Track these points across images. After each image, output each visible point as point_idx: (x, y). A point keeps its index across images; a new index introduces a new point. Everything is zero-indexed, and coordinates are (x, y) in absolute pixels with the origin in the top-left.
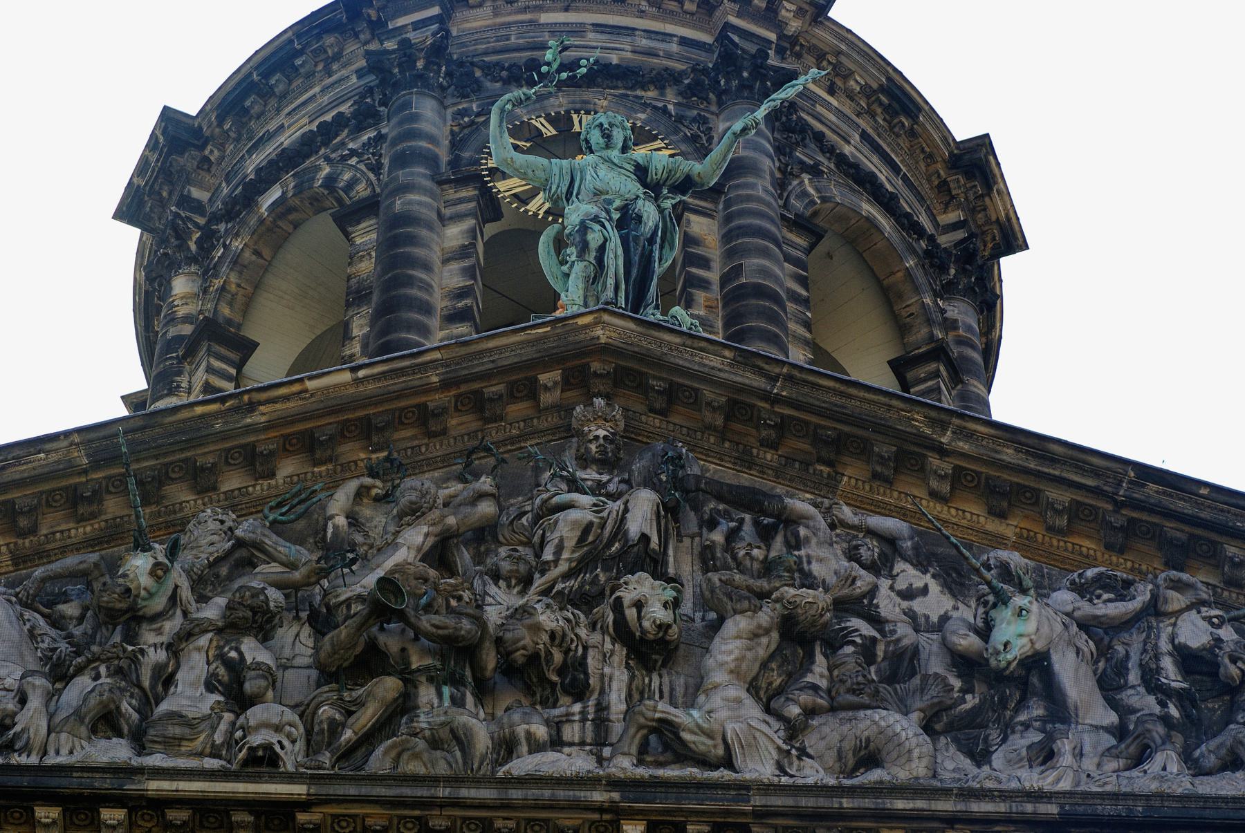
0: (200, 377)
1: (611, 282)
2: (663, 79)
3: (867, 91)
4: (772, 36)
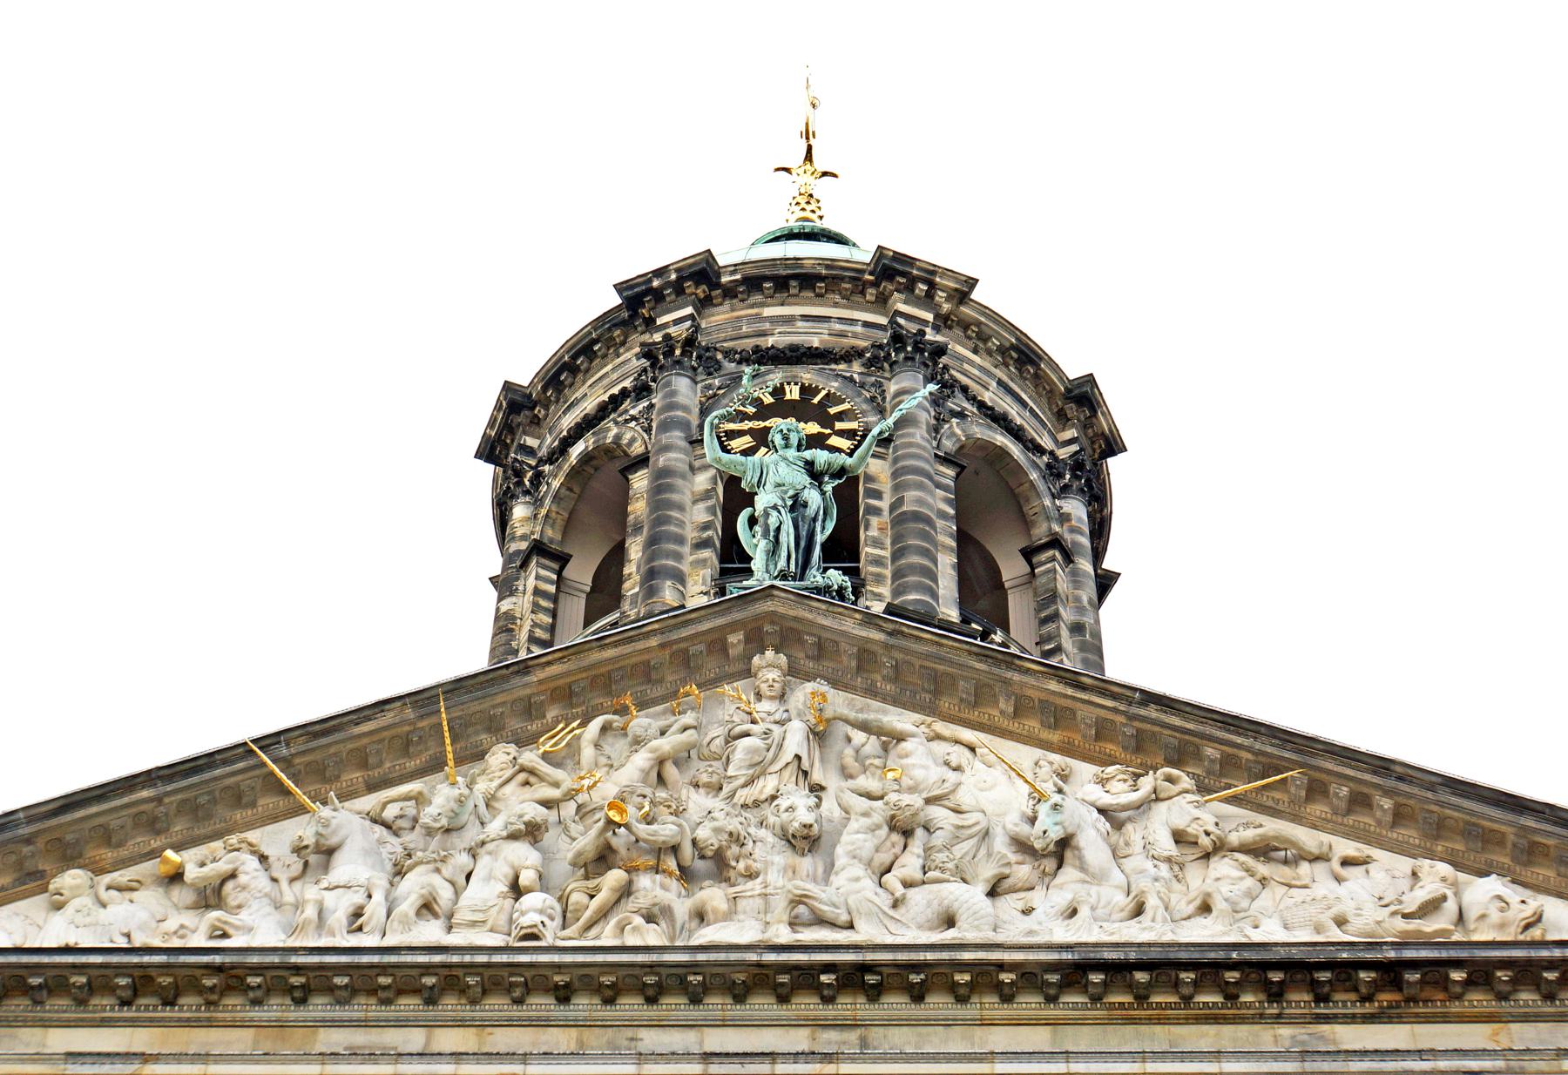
0: (531, 582)
1: (784, 554)
2: (849, 356)
3: (1002, 350)
4: (930, 317)
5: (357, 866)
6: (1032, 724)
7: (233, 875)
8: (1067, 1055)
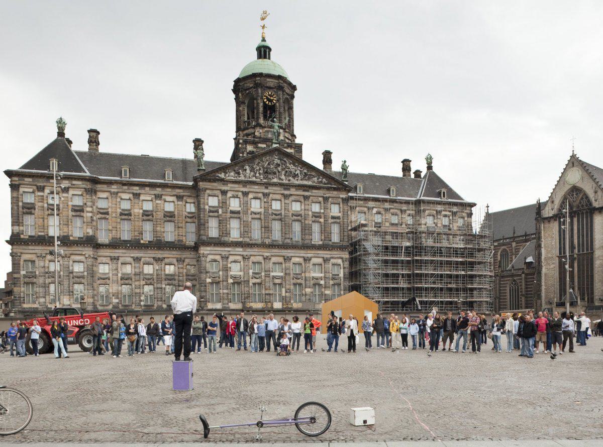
5: (248, 171)
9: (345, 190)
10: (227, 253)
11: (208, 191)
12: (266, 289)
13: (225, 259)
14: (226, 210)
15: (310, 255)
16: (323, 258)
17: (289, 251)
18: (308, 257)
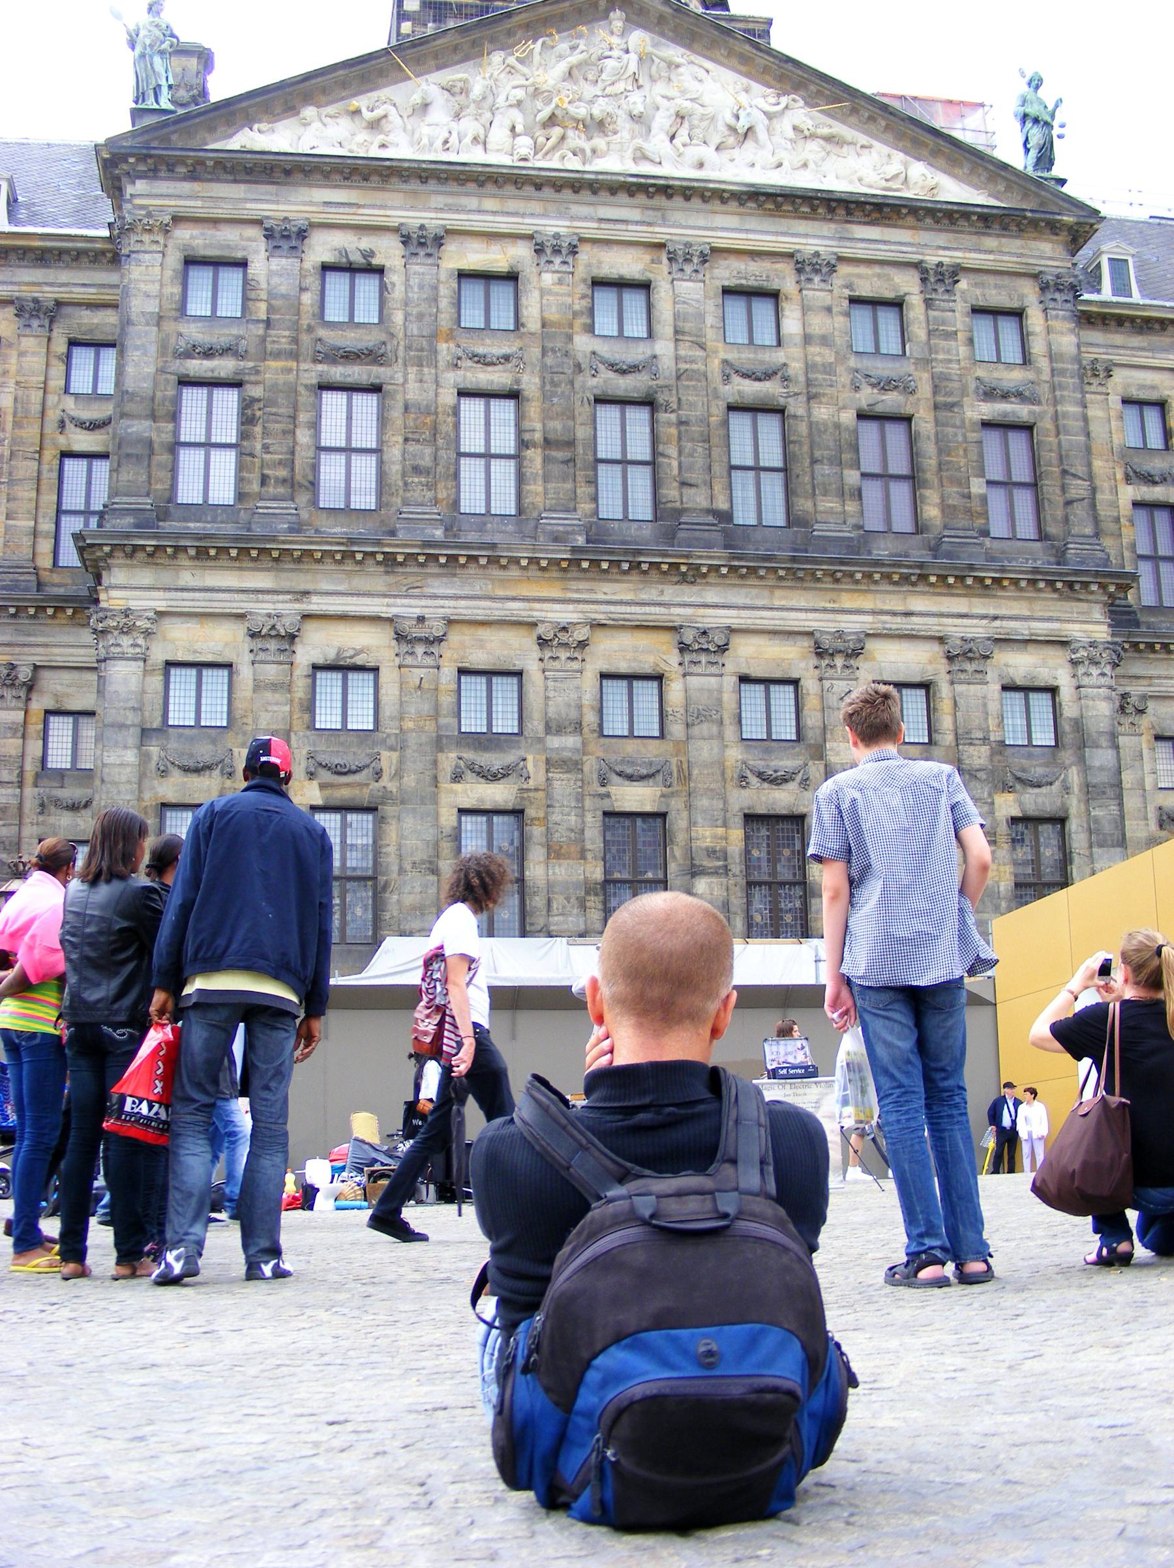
5: (439, 114)
6: (734, 62)
7: (385, 116)
8: (747, 231)
9: (1054, 227)
10: (289, 609)
11: (185, 235)
12: (554, 852)
13: (272, 645)
14: (295, 340)
15: (852, 624)
16: (941, 640)
17: (711, 595)
18: (840, 634)
